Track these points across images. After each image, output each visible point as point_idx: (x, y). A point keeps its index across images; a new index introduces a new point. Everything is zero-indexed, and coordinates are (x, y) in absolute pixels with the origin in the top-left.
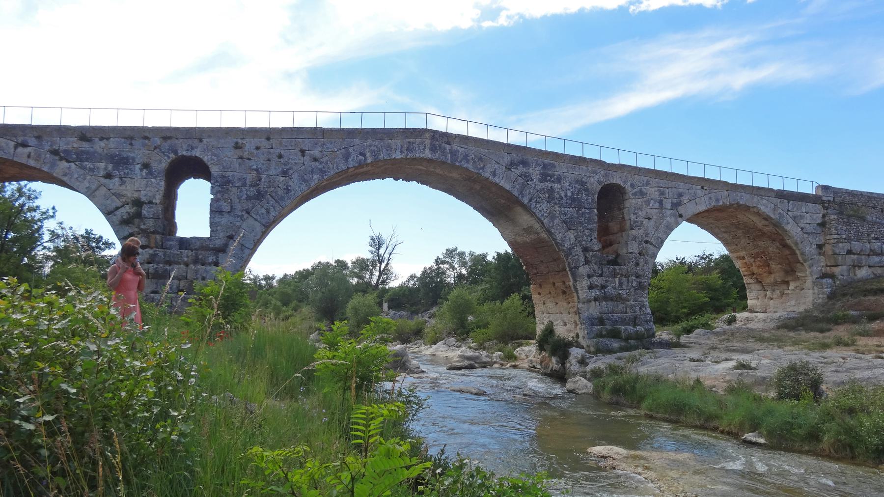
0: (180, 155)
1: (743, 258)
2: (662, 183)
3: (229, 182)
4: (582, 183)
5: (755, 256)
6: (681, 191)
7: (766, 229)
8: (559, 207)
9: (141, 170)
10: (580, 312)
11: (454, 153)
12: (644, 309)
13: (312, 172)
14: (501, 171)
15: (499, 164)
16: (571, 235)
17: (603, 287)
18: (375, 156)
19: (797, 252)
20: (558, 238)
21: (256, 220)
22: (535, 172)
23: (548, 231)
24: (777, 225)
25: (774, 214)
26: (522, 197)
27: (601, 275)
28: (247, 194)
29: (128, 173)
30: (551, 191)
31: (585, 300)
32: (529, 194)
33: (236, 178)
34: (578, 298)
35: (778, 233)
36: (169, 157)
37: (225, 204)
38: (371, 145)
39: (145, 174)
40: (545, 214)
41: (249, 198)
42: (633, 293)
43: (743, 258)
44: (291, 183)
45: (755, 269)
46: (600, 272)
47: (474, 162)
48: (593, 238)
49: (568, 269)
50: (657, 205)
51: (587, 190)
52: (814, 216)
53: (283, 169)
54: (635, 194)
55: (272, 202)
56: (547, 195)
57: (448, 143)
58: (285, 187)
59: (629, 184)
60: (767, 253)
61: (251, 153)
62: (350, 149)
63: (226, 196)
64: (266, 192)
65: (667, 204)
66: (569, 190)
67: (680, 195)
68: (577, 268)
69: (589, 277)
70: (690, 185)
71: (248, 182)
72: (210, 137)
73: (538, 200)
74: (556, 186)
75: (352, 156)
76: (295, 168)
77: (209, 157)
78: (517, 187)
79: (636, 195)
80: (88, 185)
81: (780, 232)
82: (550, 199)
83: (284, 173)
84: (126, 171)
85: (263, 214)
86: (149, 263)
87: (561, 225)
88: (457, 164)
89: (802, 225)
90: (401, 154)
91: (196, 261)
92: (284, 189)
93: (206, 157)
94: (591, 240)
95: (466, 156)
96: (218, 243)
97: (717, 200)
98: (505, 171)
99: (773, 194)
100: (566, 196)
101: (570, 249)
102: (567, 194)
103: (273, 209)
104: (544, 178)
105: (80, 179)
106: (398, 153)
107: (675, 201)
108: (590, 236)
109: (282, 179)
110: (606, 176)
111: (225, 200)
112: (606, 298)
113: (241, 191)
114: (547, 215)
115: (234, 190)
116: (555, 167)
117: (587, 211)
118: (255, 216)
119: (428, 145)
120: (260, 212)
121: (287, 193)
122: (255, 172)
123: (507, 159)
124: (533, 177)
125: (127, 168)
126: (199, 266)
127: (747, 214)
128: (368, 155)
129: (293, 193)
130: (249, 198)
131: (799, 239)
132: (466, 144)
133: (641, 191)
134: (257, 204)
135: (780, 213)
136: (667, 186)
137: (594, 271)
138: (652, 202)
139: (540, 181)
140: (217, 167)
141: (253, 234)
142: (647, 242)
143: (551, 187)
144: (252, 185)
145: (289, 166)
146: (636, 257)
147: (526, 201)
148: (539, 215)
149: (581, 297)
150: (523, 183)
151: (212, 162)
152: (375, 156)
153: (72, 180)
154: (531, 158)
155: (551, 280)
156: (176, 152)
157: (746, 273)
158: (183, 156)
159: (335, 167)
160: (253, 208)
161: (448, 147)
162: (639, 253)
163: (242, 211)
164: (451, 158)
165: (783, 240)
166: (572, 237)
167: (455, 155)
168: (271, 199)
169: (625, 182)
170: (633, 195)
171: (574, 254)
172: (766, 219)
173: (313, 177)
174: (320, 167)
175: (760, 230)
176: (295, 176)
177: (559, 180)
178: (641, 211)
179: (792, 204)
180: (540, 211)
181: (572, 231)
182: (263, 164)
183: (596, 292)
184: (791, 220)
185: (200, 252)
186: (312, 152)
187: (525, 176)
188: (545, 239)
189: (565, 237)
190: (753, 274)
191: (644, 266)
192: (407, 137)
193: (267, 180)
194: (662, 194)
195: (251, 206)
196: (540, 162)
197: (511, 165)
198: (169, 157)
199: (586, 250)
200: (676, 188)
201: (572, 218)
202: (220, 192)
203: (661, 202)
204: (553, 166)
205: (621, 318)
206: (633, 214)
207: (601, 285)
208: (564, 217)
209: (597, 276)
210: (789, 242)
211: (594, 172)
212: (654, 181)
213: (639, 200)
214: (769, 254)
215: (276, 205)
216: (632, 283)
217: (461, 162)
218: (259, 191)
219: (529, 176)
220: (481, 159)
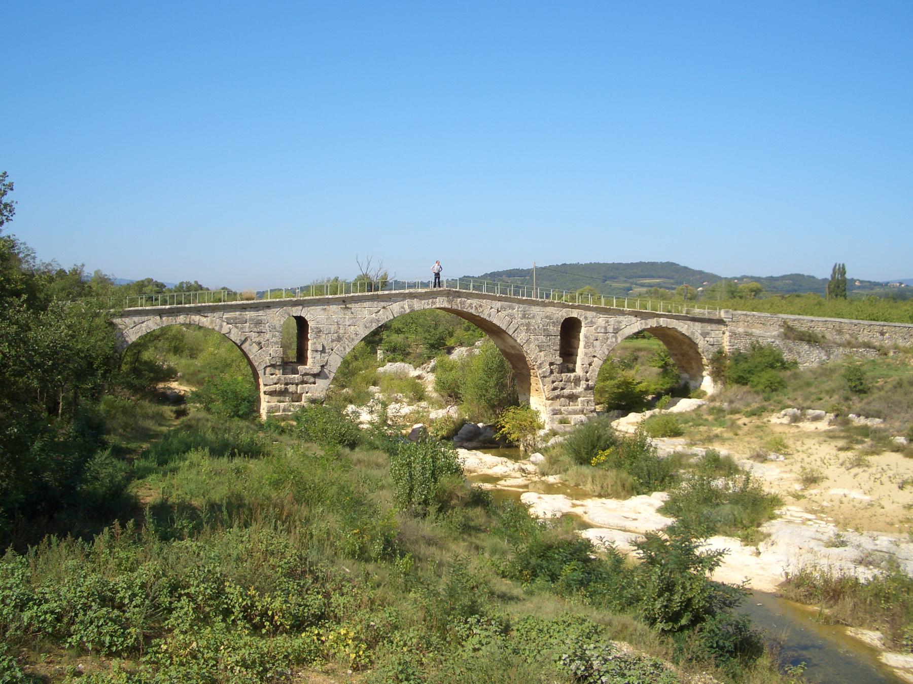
3: (320, 331)
27: (561, 381)
30: (528, 325)
44: (358, 329)
52: (717, 332)
65: (610, 329)
82: (528, 330)
86: (276, 384)
91: (303, 382)
104: (524, 317)
126: (305, 385)
130: (333, 341)
133: (591, 321)
142: (594, 356)
147: (510, 332)
177: (533, 317)
183: (557, 392)
199: (551, 364)
203: (606, 328)
215: (350, 344)
218: (339, 337)
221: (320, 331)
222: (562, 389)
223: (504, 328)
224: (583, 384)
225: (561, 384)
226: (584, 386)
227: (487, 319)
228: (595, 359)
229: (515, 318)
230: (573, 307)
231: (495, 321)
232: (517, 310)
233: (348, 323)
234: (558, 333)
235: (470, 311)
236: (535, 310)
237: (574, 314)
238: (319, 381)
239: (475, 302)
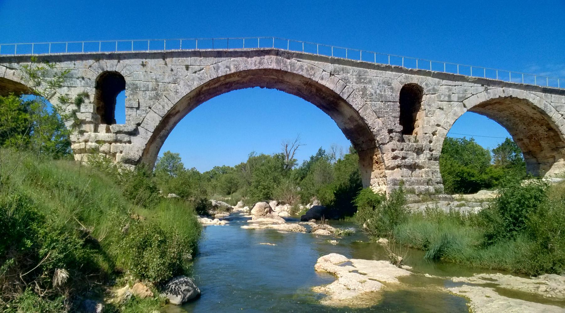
0: (105, 70)
2: (450, 83)
3: (137, 88)
4: (389, 84)
6: (465, 88)
7: (535, 116)
8: (370, 101)
9: (81, 81)
10: (386, 175)
11: (292, 65)
12: (436, 174)
13: (193, 80)
14: (326, 74)
15: (325, 71)
16: (380, 121)
17: (404, 158)
18: (236, 68)
19: (559, 133)
20: (370, 123)
23: (362, 119)
24: (542, 112)
25: (540, 104)
26: (342, 94)
27: (402, 149)
28: (149, 96)
29: (72, 84)
30: (365, 89)
31: (390, 167)
32: (348, 92)
33: (142, 85)
36: (98, 72)
37: (135, 102)
38: (233, 61)
39: (83, 84)
40: (360, 106)
41: (151, 99)
42: (427, 162)
43: (522, 140)
45: (531, 148)
46: (401, 147)
47: (308, 71)
48: (396, 123)
50: (446, 99)
51: (392, 88)
53: (173, 78)
54: (429, 91)
55: (166, 100)
56: (361, 93)
57: (288, 58)
58: (175, 90)
59: (424, 83)
60: (538, 135)
61: (152, 68)
62: (220, 64)
63: (135, 97)
64: (162, 94)
65: (454, 97)
66: (378, 88)
69: (393, 150)
70: (473, 84)
71: (150, 87)
72: (125, 58)
73: (355, 96)
74: (369, 86)
75: (221, 69)
76: (181, 77)
77: (124, 71)
78: (339, 87)
79: (430, 91)
81: (545, 118)
82: (364, 95)
84: (71, 82)
85: (160, 109)
87: (371, 113)
88: (295, 72)
89: (562, 113)
90: (255, 66)
91: (116, 141)
92: (174, 92)
93: (122, 72)
94: (395, 124)
95: (302, 66)
96: (131, 128)
97: (495, 95)
98: (330, 77)
100: (376, 93)
101: (378, 131)
102: (376, 91)
103: (167, 106)
104: (360, 79)
106: (253, 65)
107: (461, 95)
108: (394, 121)
110: (407, 78)
111: (135, 100)
113: (146, 93)
114: (361, 107)
115: (141, 93)
116: (367, 72)
117: (392, 103)
120: (158, 108)
121: (176, 94)
122: (155, 81)
124: (351, 80)
125: (72, 80)
126: (119, 144)
127: (519, 105)
128: (232, 67)
129: (180, 94)
130: (151, 99)
131: (559, 123)
133: (434, 89)
134: (156, 102)
135: (545, 104)
136: (454, 85)
137: (397, 147)
138: (443, 96)
139: (356, 83)
140: (129, 78)
141: (154, 122)
142: (438, 125)
143: (365, 87)
144: (153, 90)
146: (430, 137)
147: (345, 97)
148: (354, 106)
150: (343, 85)
151: (127, 75)
152: (236, 68)
156: (103, 69)
158: (107, 72)
159: (209, 76)
160: (153, 104)
161: (288, 61)
162: (432, 134)
163: (146, 107)
164: (290, 68)
165: (548, 124)
166: (381, 122)
167: (294, 66)
168: (165, 98)
169: (421, 83)
170: (427, 91)
171: (381, 135)
173: (193, 83)
174: (199, 76)
175: (532, 118)
176: (182, 83)
177: (370, 82)
178: (434, 103)
179: (554, 97)
180: (356, 104)
182: (160, 75)
183: (398, 162)
184: (553, 109)
185: (118, 135)
187: (345, 80)
189: (375, 122)
190: (530, 151)
191: (436, 143)
193: (163, 86)
194: (450, 90)
195: (152, 103)
197: (334, 72)
198: (98, 72)
199: (390, 131)
200: (461, 86)
201: (380, 108)
202: (131, 94)
203: (449, 96)
204: (367, 72)
205: (417, 180)
206: (428, 105)
207: (403, 156)
208: (374, 108)
209: (399, 150)
210: (552, 126)
211: (396, 75)
212: (444, 82)
213: (433, 95)
214: (539, 135)
215: (170, 103)
216: (426, 155)
217: (298, 70)
219: (347, 79)
220: (312, 68)
221: (137, 88)
222: (404, 158)
223: (338, 92)
224: (427, 153)
225: (401, 154)
226: (429, 156)
227: (320, 82)
228: (439, 128)
229: (349, 82)
230: (412, 72)
231: (331, 86)
232: (352, 72)
233: (167, 80)
234: (398, 99)
235: (301, 73)
236: (371, 73)
237: (415, 79)
238: (133, 139)
239: (306, 63)
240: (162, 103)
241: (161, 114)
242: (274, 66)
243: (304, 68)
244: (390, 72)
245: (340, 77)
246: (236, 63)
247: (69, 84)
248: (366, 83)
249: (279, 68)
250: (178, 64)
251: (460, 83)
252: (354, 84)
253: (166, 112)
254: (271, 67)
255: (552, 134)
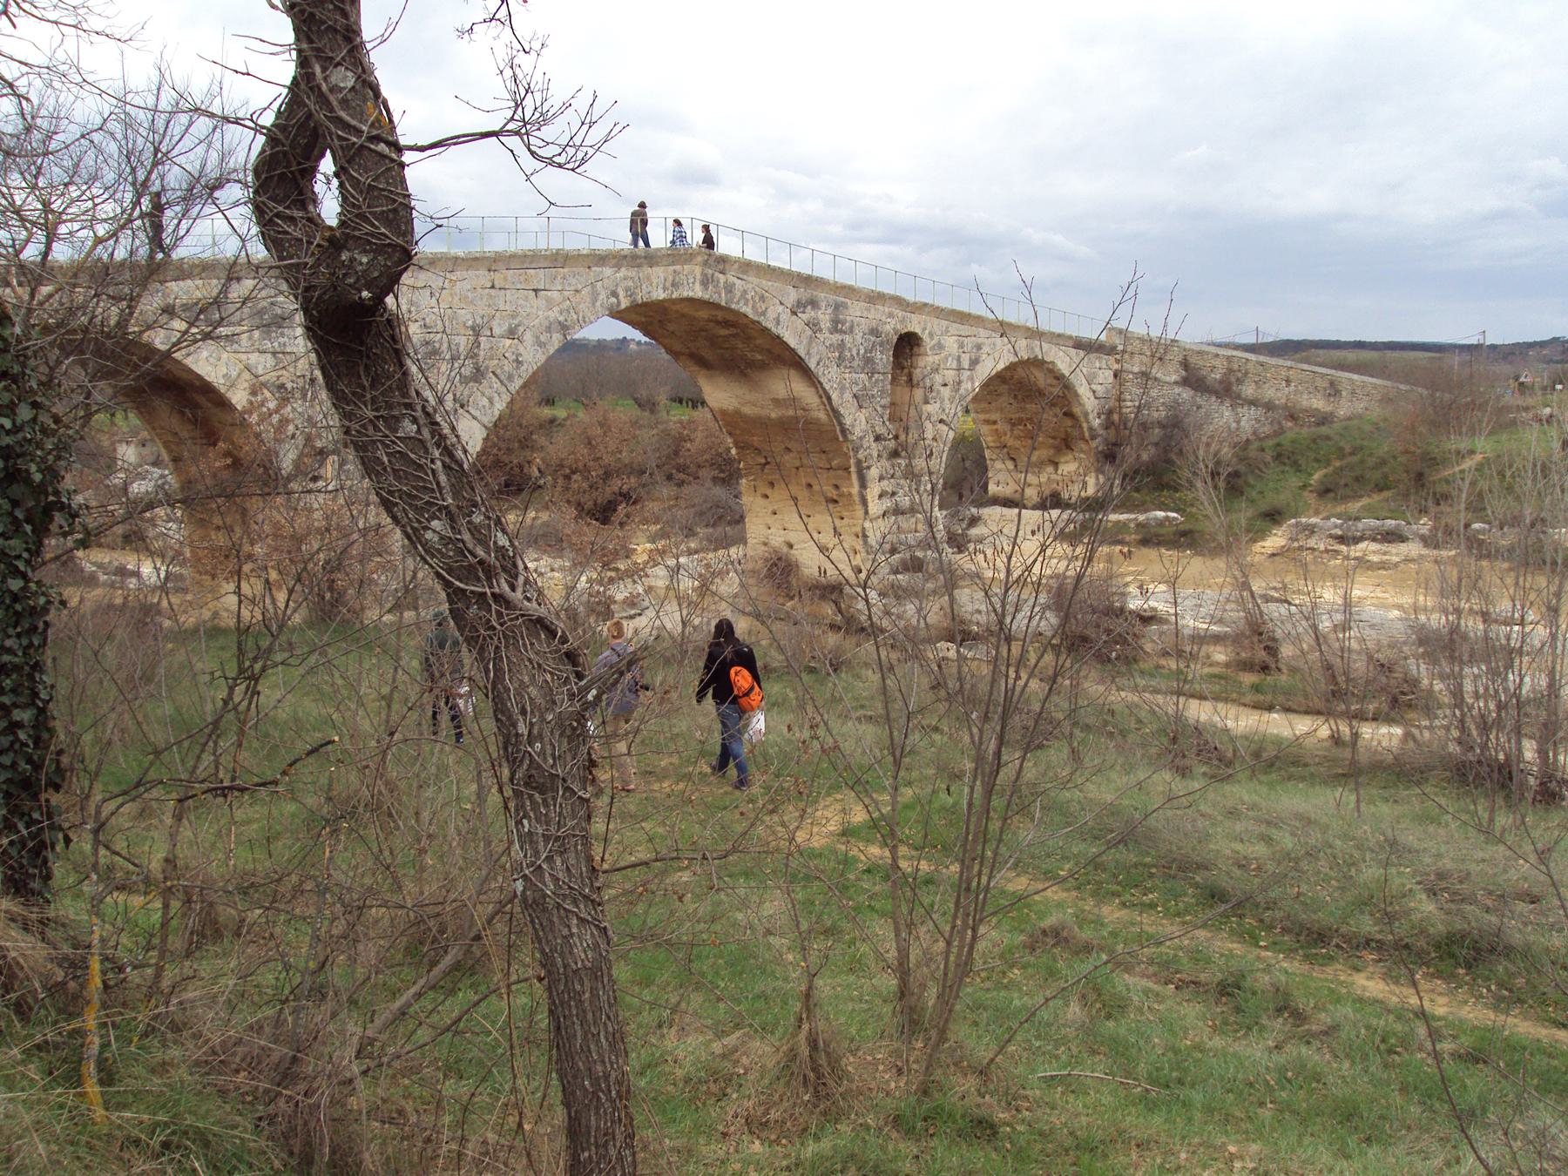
1: (995, 422)
2: (965, 330)
5: (1013, 424)
6: (980, 341)
11: (729, 289)
14: (786, 316)
16: (862, 416)
21: (475, 418)
22: (824, 317)
24: (1067, 385)
30: (842, 345)
34: (866, 512)
35: (1064, 397)
43: (995, 422)
44: (521, 350)
45: (1010, 442)
49: (853, 469)
61: (463, 298)
64: (487, 368)
65: (966, 364)
67: (979, 347)
68: (869, 468)
74: (847, 338)
80: (225, 371)
83: (512, 333)
84: (282, 340)
88: (733, 306)
89: (1094, 387)
95: (745, 292)
99: (1071, 344)
101: (861, 438)
105: (211, 360)
109: (508, 342)
112: (898, 511)
118: (473, 412)
119: (699, 277)
121: (518, 368)
123: (792, 296)
125: (282, 335)
128: (622, 294)
132: (745, 272)
142: (941, 421)
145: (519, 319)
147: (812, 365)
148: (827, 387)
149: (871, 512)
153: (200, 363)
154: (821, 295)
155: (804, 481)
157: (991, 444)
168: (494, 379)
169: (924, 329)
172: (1057, 378)
174: (561, 319)
176: (528, 337)
181: (863, 411)
183: (887, 503)
184: (1084, 381)
186: (549, 293)
188: (818, 419)
192: (673, 263)
193: (488, 346)
194: (961, 346)
196: (831, 302)
199: (878, 438)
201: (865, 388)
204: (845, 306)
208: (855, 389)
210: (1077, 410)
211: (890, 315)
212: (955, 328)
217: (738, 303)
223: (802, 353)
227: (774, 330)
229: (821, 330)
237: (915, 325)
239: (753, 283)
240: (488, 392)
241: (485, 420)
242: (697, 292)
243: (749, 297)
244: (881, 308)
245: (804, 317)
246: (630, 283)
247: (276, 344)
248: (845, 333)
249: (707, 297)
250: (519, 286)
251: (974, 330)
252: (827, 335)
253: (497, 413)
254: (691, 294)
255: (1069, 422)
